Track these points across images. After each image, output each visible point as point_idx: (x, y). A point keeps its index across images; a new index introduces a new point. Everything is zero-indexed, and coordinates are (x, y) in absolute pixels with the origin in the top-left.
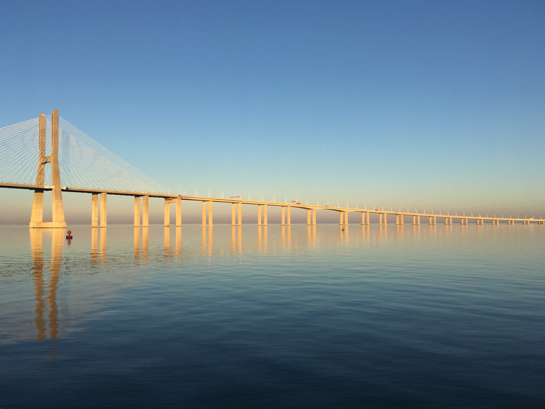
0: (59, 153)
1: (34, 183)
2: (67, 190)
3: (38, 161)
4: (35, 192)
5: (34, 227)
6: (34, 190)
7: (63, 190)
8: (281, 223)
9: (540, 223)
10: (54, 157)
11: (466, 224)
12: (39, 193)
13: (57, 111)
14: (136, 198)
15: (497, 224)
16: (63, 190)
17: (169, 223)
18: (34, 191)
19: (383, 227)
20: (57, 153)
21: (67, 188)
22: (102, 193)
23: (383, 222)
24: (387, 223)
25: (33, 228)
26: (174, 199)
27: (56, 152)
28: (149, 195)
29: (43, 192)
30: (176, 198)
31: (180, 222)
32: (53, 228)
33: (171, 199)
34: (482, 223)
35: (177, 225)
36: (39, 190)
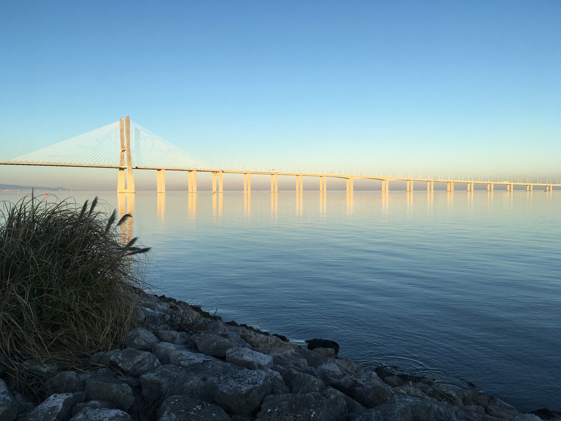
0: (130, 144)
1: (118, 165)
2: (137, 168)
3: (120, 150)
7: (133, 168)
8: (271, 190)
10: (127, 147)
11: (530, 191)
12: (121, 171)
13: (128, 117)
14: (189, 172)
16: (133, 168)
17: (216, 190)
18: (119, 169)
19: (430, 193)
20: (129, 144)
21: (136, 167)
23: (430, 190)
24: (434, 190)
29: (124, 170)
30: (219, 172)
35: (219, 191)
36: (121, 169)
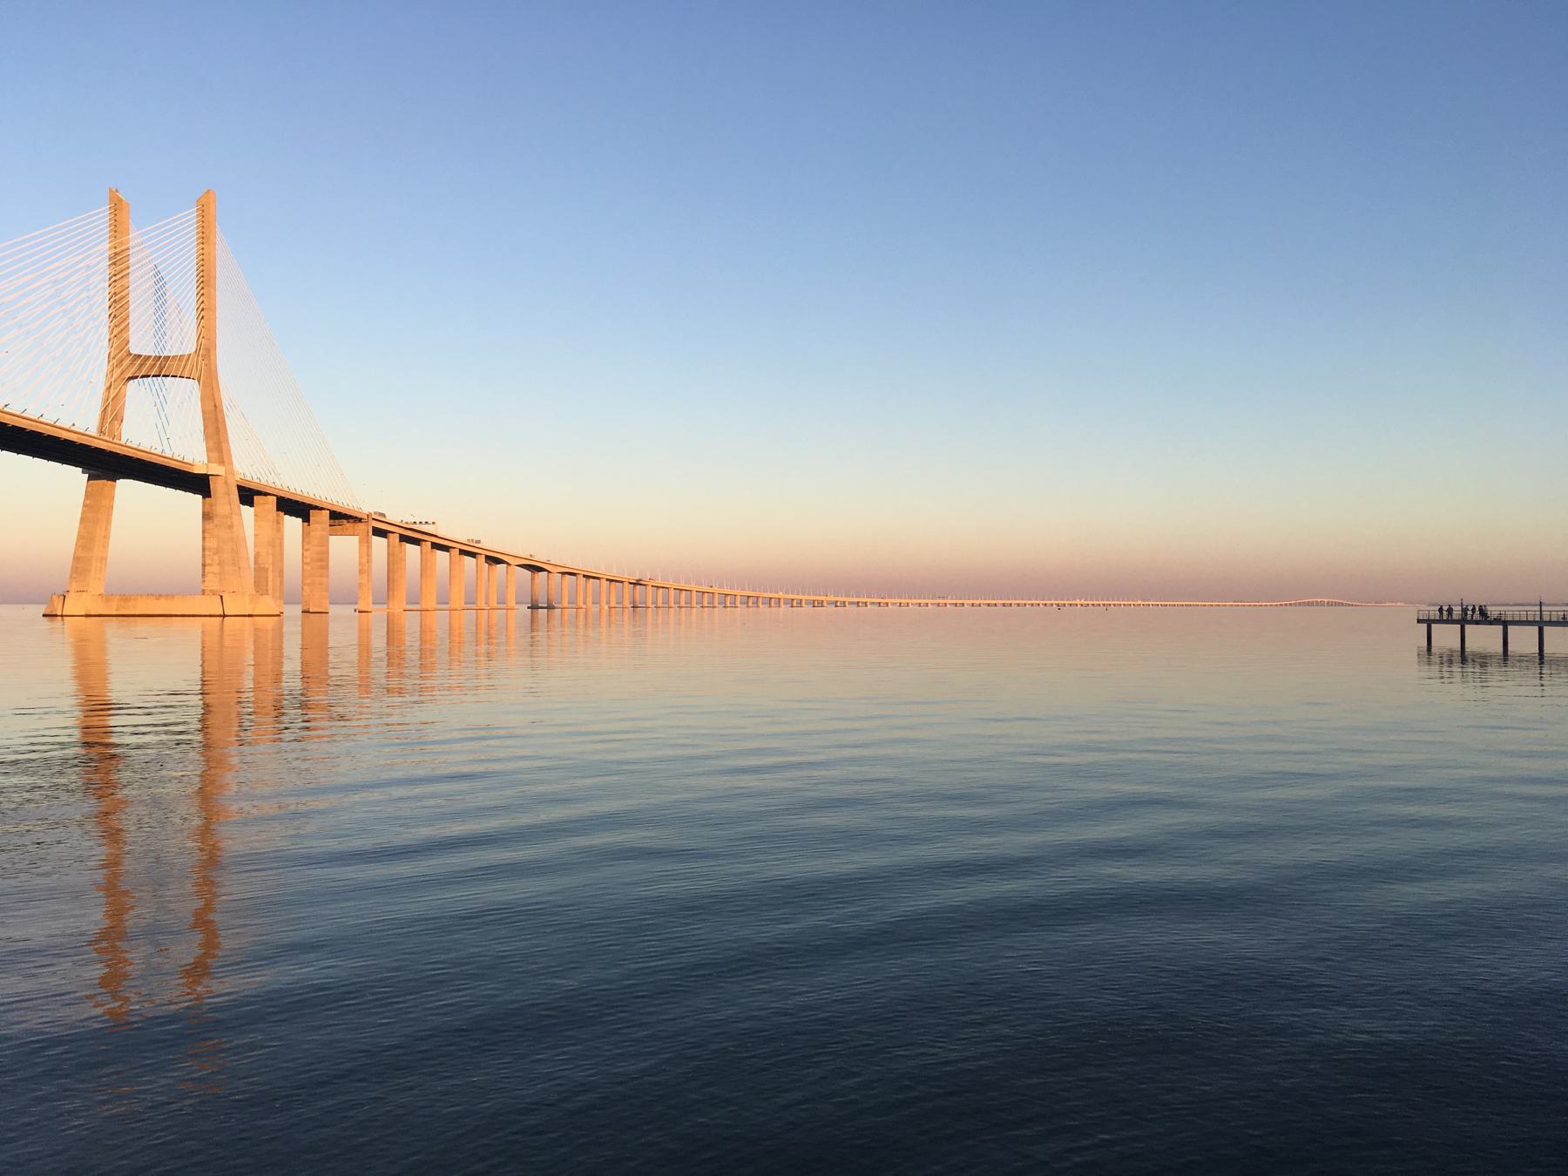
4: (89, 480)
5: (93, 613)
6: (87, 475)
9: (795, 604)
15: (758, 607)
22: (266, 494)
25: (87, 616)
26: (348, 525)
27: (206, 349)
28: (332, 509)
30: (360, 520)
31: (370, 601)
32: (224, 616)
33: (345, 521)
34: (738, 604)
